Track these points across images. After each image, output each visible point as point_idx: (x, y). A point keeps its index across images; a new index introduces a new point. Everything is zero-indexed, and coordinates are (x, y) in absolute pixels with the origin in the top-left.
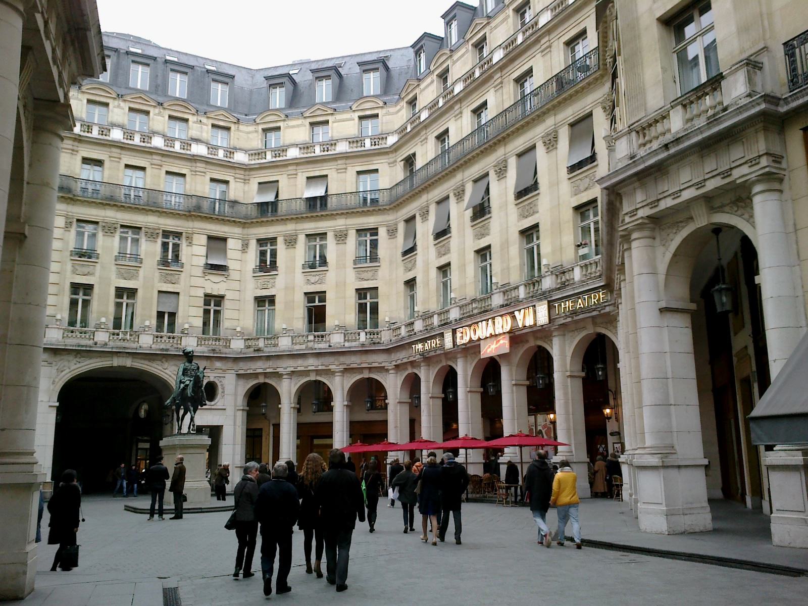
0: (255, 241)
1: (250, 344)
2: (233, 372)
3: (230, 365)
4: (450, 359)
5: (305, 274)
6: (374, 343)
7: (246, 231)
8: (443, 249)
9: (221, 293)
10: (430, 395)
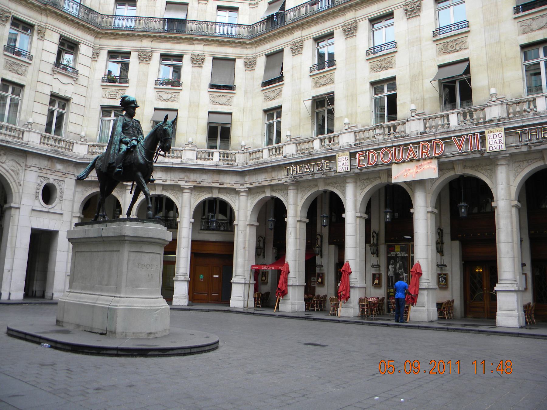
0: (106, 52)
1: (94, 151)
2: (73, 177)
3: (71, 169)
4: (330, 184)
5: (157, 90)
6: (228, 164)
7: (98, 41)
8: (324, 79)
9: (68, 95)
10: (298, 219)
